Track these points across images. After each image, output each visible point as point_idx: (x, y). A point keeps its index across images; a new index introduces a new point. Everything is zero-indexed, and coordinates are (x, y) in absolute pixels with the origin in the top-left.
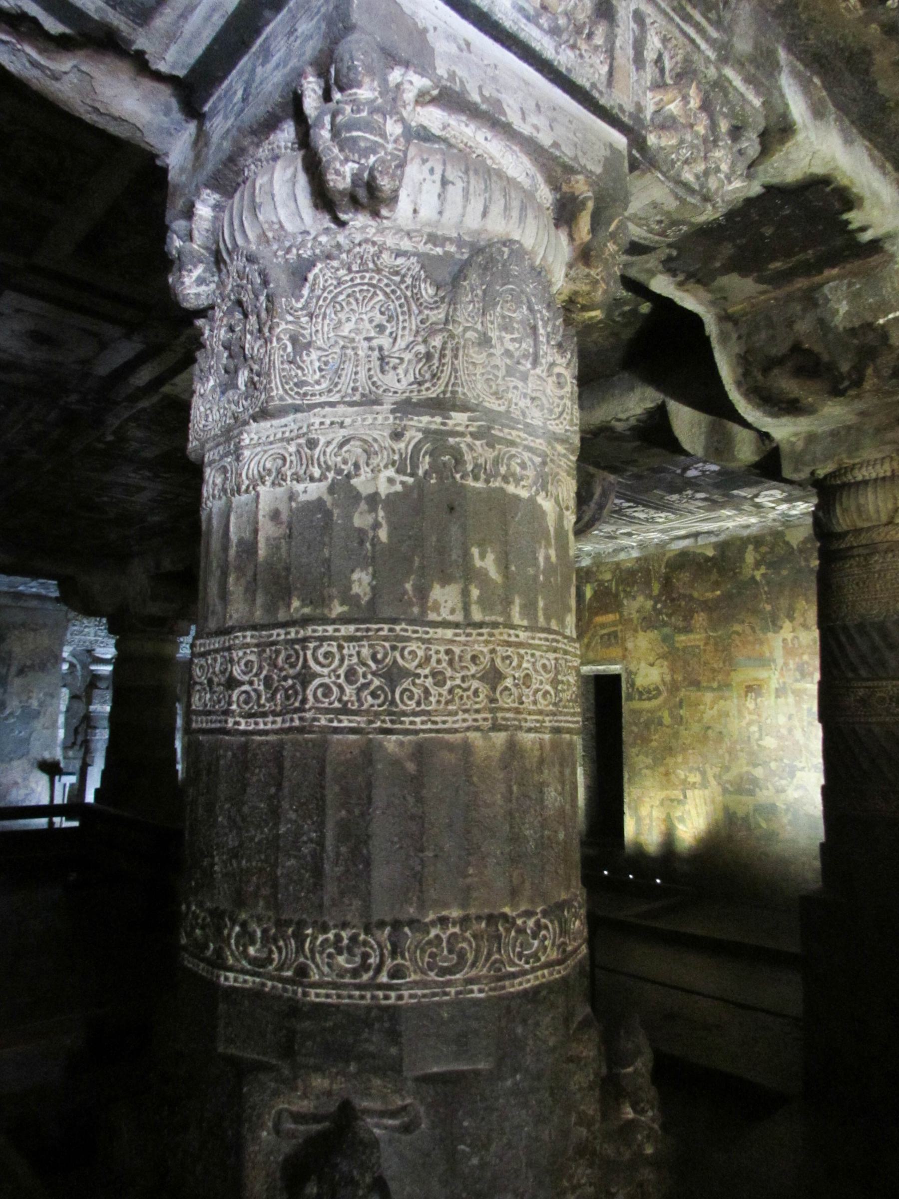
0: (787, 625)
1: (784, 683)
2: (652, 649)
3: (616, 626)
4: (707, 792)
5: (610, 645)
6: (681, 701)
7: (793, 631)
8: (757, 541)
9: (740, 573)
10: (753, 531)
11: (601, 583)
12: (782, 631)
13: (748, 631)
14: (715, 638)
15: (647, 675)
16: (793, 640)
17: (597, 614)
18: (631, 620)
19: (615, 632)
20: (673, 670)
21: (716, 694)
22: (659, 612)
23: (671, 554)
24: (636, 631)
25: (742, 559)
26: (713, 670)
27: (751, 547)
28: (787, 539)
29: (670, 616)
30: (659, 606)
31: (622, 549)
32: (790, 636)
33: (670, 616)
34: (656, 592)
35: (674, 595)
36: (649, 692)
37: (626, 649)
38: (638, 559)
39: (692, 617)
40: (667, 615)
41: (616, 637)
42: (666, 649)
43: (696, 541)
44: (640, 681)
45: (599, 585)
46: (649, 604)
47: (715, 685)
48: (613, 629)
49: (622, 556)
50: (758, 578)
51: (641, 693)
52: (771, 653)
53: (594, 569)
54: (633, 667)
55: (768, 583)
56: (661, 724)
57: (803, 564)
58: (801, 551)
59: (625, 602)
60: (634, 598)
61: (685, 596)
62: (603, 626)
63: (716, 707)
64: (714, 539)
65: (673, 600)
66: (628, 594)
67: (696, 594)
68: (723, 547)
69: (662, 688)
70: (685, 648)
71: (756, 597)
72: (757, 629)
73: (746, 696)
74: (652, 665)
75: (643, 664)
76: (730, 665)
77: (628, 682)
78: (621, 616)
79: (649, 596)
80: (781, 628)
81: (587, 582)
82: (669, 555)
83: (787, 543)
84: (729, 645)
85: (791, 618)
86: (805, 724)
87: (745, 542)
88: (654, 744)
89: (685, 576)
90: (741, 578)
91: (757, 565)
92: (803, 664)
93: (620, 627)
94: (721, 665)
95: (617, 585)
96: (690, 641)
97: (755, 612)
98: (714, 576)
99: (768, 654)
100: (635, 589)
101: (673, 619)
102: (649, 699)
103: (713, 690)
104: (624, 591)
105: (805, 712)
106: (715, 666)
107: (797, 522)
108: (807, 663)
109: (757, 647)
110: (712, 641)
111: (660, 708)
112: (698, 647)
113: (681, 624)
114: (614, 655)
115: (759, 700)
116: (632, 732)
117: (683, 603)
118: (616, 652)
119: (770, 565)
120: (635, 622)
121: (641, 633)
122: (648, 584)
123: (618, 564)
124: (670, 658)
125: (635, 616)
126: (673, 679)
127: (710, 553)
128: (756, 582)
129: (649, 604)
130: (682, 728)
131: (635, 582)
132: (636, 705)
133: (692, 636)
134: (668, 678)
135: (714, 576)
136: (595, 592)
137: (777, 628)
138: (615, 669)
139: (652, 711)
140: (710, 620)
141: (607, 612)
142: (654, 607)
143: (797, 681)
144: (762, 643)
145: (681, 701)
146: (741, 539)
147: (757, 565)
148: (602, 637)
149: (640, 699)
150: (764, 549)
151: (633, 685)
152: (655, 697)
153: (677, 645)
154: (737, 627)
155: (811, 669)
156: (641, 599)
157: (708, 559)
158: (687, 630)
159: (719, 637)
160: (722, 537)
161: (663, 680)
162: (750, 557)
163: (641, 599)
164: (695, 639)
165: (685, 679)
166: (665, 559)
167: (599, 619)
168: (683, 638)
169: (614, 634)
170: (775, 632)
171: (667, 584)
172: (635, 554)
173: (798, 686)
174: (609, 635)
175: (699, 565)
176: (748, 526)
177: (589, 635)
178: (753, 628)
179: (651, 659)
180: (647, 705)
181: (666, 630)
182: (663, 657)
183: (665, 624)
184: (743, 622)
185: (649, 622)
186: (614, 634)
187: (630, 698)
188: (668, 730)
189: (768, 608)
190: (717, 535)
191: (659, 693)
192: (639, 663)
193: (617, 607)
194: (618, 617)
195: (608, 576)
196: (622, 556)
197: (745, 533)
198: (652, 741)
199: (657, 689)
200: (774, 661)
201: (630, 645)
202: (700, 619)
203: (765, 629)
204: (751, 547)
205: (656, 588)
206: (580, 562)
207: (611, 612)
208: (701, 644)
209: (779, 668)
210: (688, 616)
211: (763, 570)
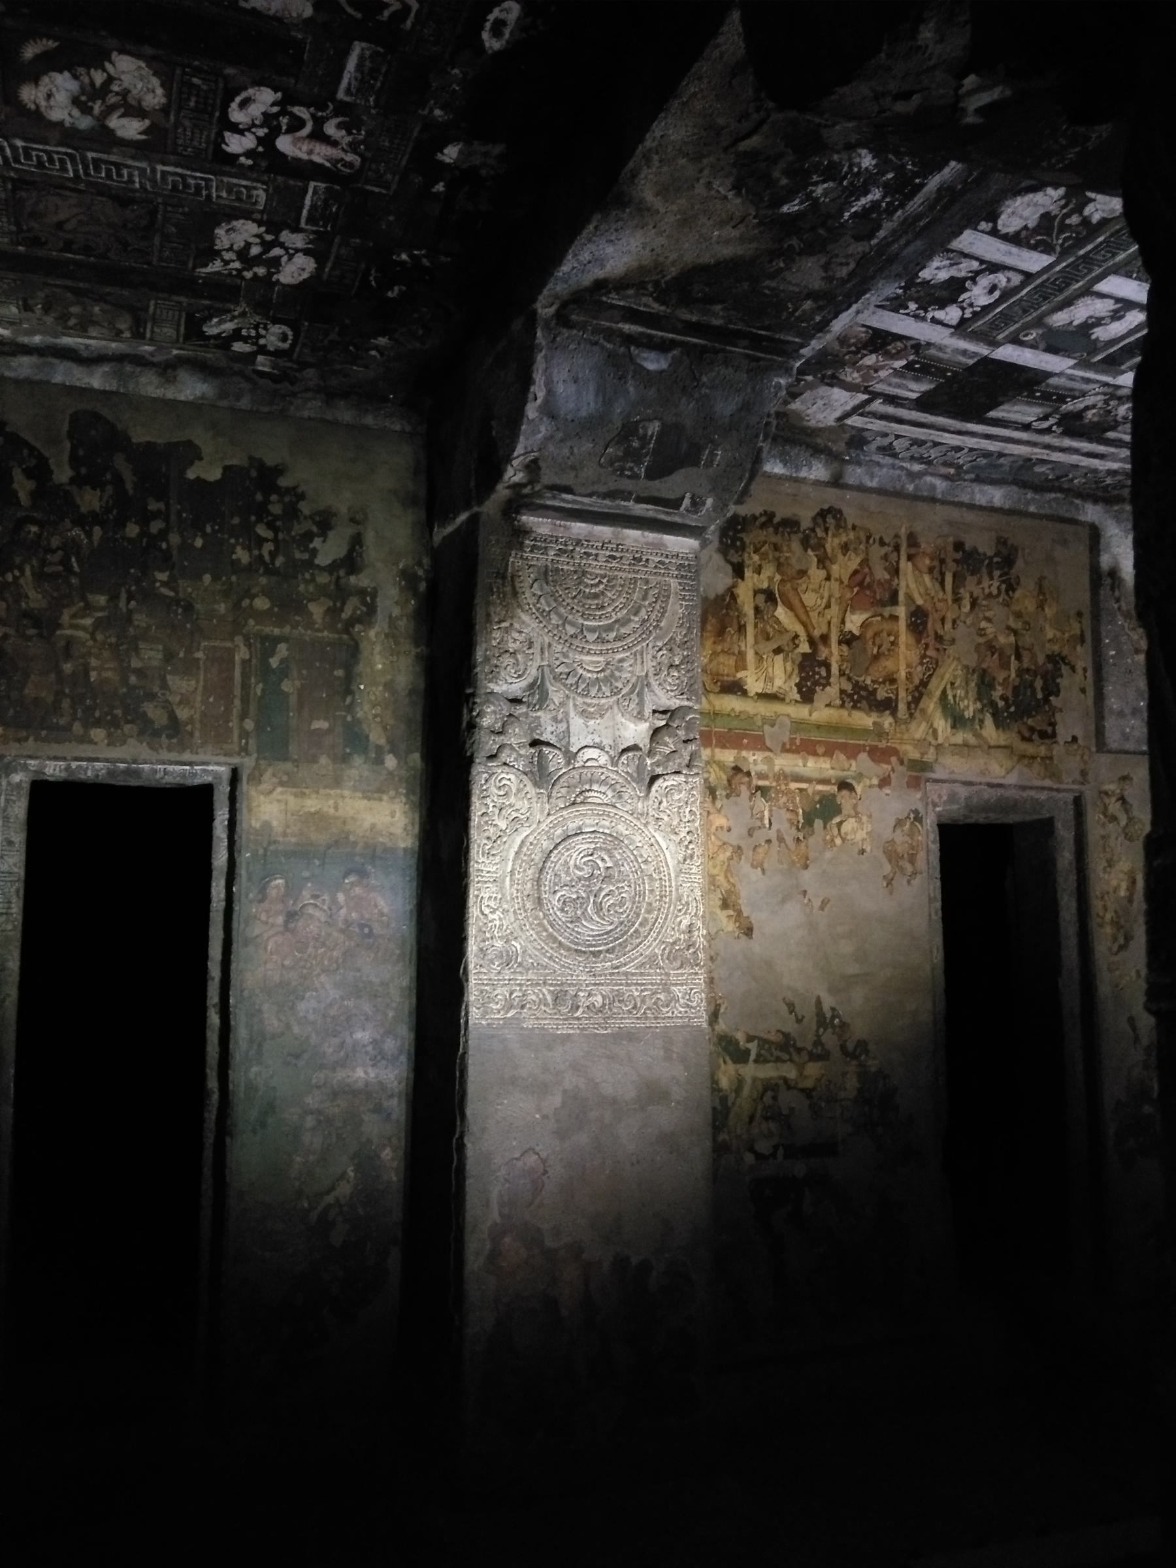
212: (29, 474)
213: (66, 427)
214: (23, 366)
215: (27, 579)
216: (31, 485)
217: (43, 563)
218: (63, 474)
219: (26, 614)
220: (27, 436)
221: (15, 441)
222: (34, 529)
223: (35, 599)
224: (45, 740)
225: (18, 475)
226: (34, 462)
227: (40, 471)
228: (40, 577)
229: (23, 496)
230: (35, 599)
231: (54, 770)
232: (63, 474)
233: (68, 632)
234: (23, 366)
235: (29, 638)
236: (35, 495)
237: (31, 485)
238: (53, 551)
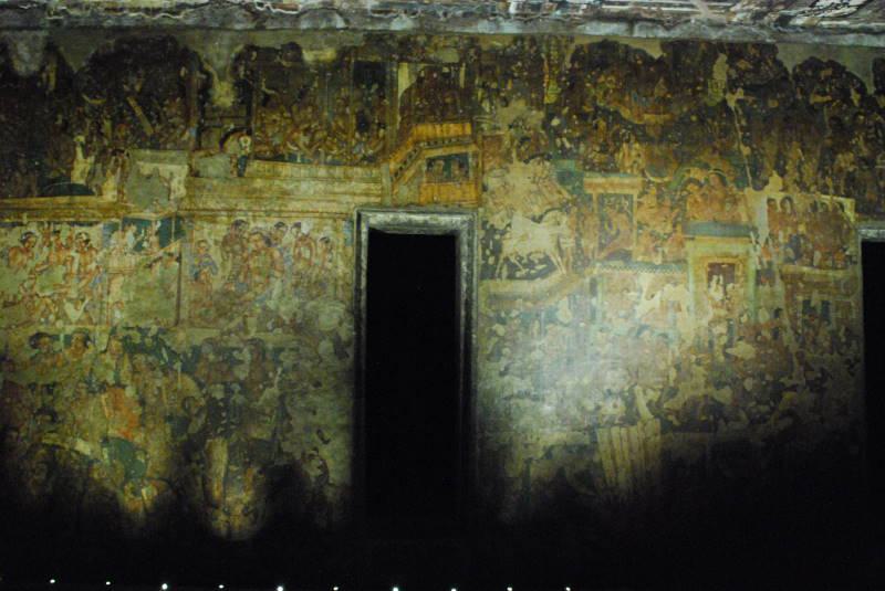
0: (775, 180)
1: (770, 263)
2: (539, 192)
3: (466, 145)
4: (633, 429)
5: (449, 178)
6: (593, 284)
7: (785, 189)
8: (735, 51)
9: (704, 92)
10: (730, 35)
11: (434, 66)
12: (767, 188)
13: (714, 180)
14: (659, 186)
15: (525, 237)
16: (783, 202)
17: (420, 120)
18: (499, 139)
19: (465, 156)
20: (579, 234)
21: (660, 274)
22: (558, 133)
23: (587, 41)
24: (507, 157)
25: (709, 74)
26: (654, 236)
27: (723, 58)
28: (779, 57)
29: (576, 141)
30: (555, 122)
31: (484, 16)
32: (778, 197)
33: (576, 141)
34: (550, 98)
35: (587, 109)
36: (530, 265)
37: (485, 189)
38: (517, 38)
39: (618, 150)
40: (570, 140)
41: (463, 164)
42: (567, 196)
43: (631, 30)
44: (510, 246)
45: (431, 71)
46: (537, 116)
47: (658, 260)
48: (455, 150)
49: (483, 27)
50: (732, 104)
51: (513, 268)
52: (750, 218)
53: (421, 39)
54: (497, 220)
55: (748, 115)
56: (552, 320)
57: (799, 97)
58: (796, 77)
59: (486, 106)
60: (506, 102)
61: (606, 113)
62: (434, 143)
63: (658, 295)
64: (661, 33)
65: (583, 116)
66: (491, 94)
67: (626, 113)
68: (677, 48)
69: (555, 259)
70: (602, 197)
71: (725, 132)
72: (728, 179)
73: (710, 279)
74: (538, 220)
75: (518, 218)
76: (685, 230)
77: (485, 247)
78: (476, 126)
79: (539, 105)
80: (766, 183)
81: (402, 59)
82: (578, 42)
83: (779, 64)
84: (683, 199)
85: (782, 173)
86: (799, 323)
87: (716, 48)
88: (537, 355)
89: (609, 81)
90: (706, 100)
91: (732, 86)
92: (797, 238)
93: (472, 149)
94: (669, 228)
95: (468, 74)
96: (612, 185)
97: (725, 153)
98: (660, 89)
99: (744, 219)
100: (509, 87)
101: (582, 148)
102: (529, 277)
103: (656, 267)
104: (483, 86)
105: (800, 308)
106: (662, 233)
107: (793, 37)
108: (803, 235)
109: (728, 207)
110: (653, 191)
111: (551, 292)
112: (626, 197)
113: (596, 157)
114: (458, 195)
115: (730, 286)
116: (494, 333)
117: (602, 124)
118: (456, 191)
119: (748, 89)
120: (507, 142)
121: (517, 165)
122: (536, 83)
123: (473, 40)
124: (575, 209)
125: (505, 133)
126: (578, 245)
127: (656, 53)
128: (728, 110)
129: (537, 116)
130: (594, 328)
131: (508, 75)
132: (502, 286)
133: (615, 179)
134: (568, 244)
135: (660, 89)
136: (420, 80)
137: (760, 185)
138: (446, 221)
139: (536, 300)
140: (651, 157)
141: (443, 119)
142: (546, 125)
143: (788, 261)
144: (735, 202)
145: (593, 284)
146: (708, 43)
147: (732, 86)
148: (431, 162)
149: (511, 277)
150: (742, 64)
151: (497, 251)
152: (543, 275)
153: (589, 191)
154: (696, 173)
155: (810, 246)
156: (519, 106)
157: (649, 61)
158: (608, 168)
159: (667, 185)
160: (676, 33)
161: (558, 246)
162: (721, 71)
163: (519, 106)
164: (625, 183)
165: (602, 247)
166: (572, 47)
167: (426, 130)
168: (599, 179)
169: (462, 161)
170: (758, 188)
171: (572, 86)
172: (510, 28)
173: (791, 268)
174: (448, 159)
175: (635, 68)
176: (721, 26)
177: (400, 156)
178: (722, 179)
179: (537, 211)
180: (525, 287)
181: (569, 164)
182: (564, 208)
183: (565, 154)
184: (706, 167)
185: (531, 148)
186: (462, 161)
187: (489, 273)
188: (565, 330)
189: (746, 151)
190: (667, 29)
191: (551, 268)
192: (510, 216)
193: (471, 114)
194: (468, 130)
195: (451, 56)
196: (483, 27)
197: (714, 35)
198: (534, 348)
199: (546, 260)
200: (755, 230)
201: (492, 182)
202: (632, 153)
203: (741, 182)
204: (723, 58)
205: (551, 94)
206: (390, 21)
207: (453, 121)
208: (635, 193)
209: (762, 240)
210: (610, 146)
211: (740, 94)
212: (858, 91)
213: (871, 67)
214: (850, 39)
215: (861, 143)
216: (858, 96)
217: (867, 134)
218: (871, 90)
219: (863, 159)
220: (855, 73)
221: (851, 76)
222: (862, 117)
223: (865, 152)
224: (876, 219)
225: (853, 92)
226: (858, 85)
227: (862, 90)
228: (867, 140)
229: (856, 102)
230: (865, 152)
231: (872, 234)
232: (871, 90)
233: (880, 167)
234: (850, 39)
235: (864, 171)
236: (861, 101)
237: (858, 96)
238: (870, 127)
